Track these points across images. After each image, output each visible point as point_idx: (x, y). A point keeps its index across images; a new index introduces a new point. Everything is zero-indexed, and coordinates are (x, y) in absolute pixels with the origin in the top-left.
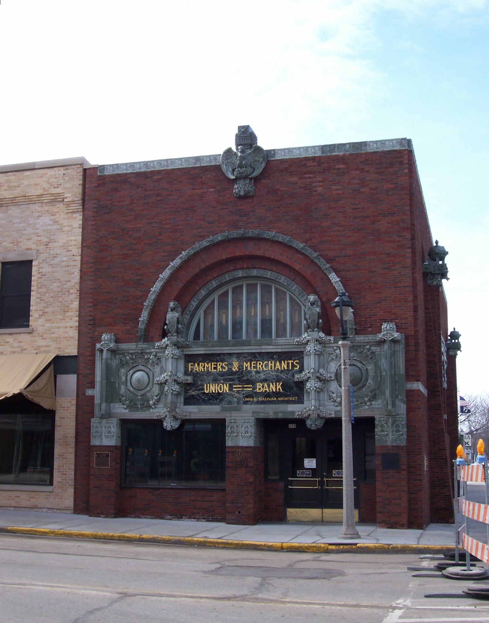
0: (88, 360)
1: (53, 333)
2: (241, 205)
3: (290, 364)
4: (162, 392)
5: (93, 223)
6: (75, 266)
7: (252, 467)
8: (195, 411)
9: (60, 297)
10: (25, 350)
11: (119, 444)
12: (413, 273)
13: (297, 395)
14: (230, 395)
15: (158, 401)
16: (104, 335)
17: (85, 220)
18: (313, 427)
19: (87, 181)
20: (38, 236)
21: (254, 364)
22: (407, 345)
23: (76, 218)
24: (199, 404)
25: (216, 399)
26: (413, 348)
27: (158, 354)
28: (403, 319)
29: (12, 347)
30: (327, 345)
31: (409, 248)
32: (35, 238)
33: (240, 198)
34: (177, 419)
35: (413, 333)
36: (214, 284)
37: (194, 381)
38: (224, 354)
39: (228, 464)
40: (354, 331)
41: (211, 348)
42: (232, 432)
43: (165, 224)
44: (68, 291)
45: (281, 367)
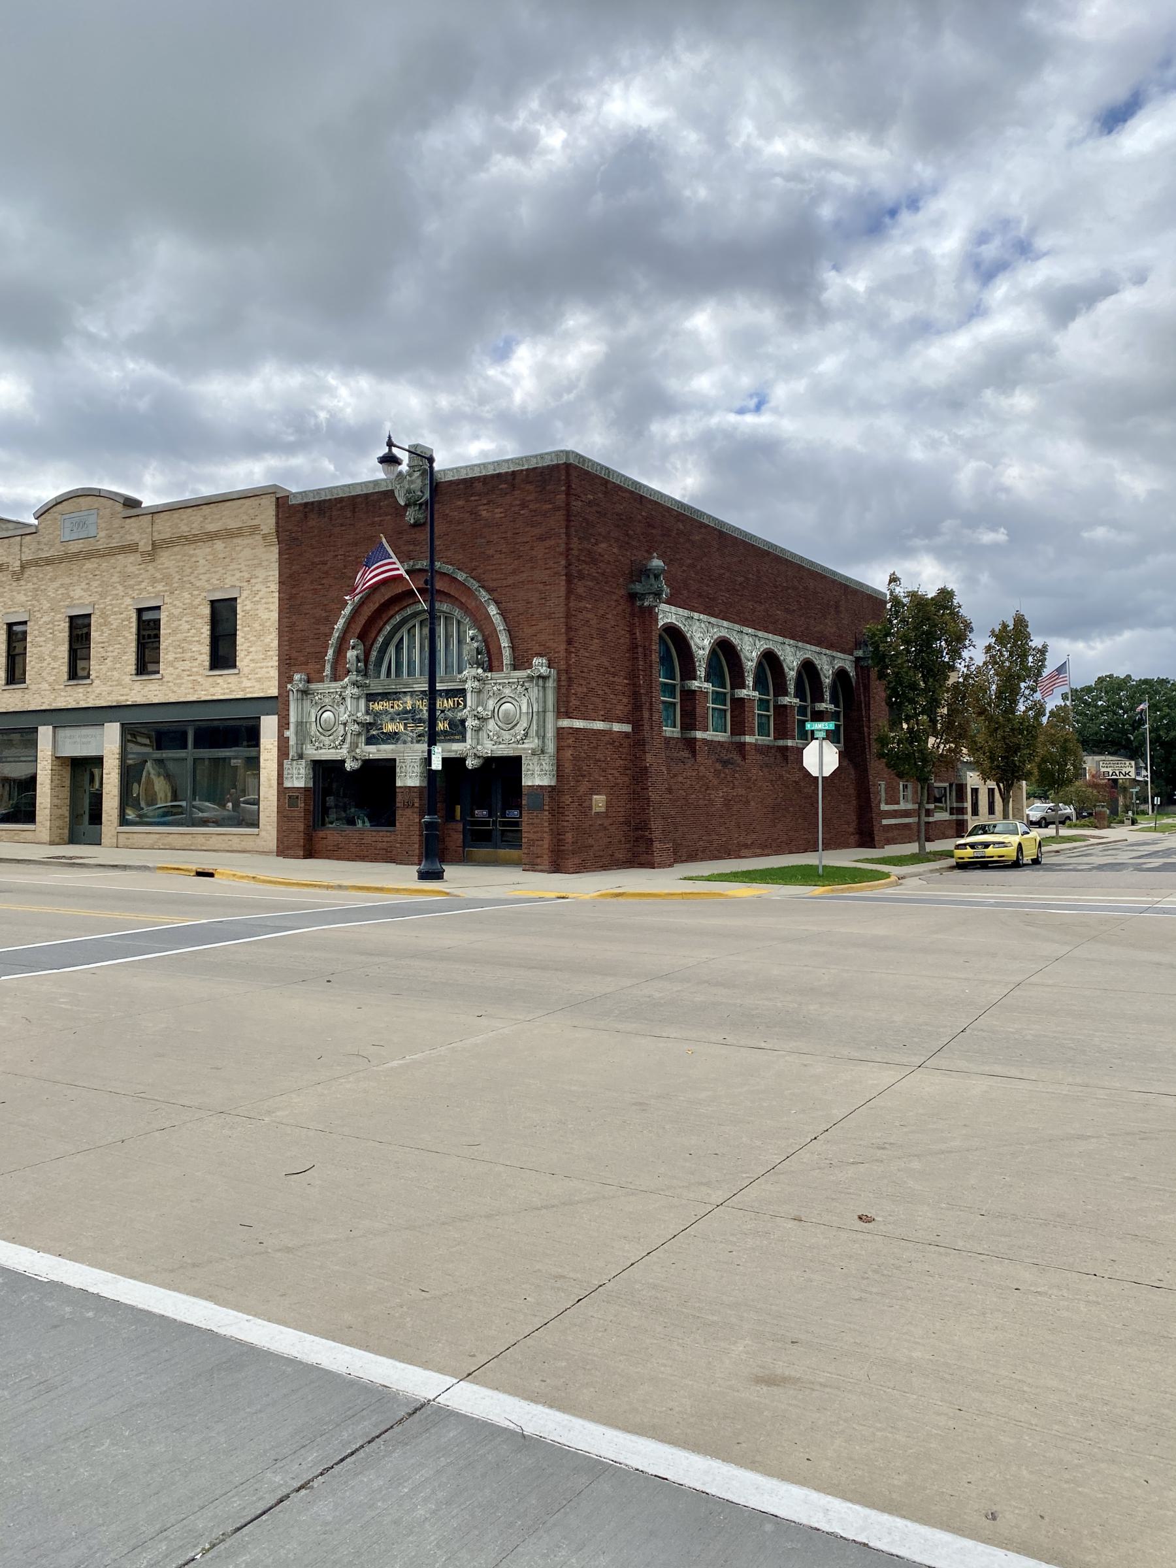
8: (374, 752)
15: (343, 741)
17: (280, 553)
22: (559, 680)
32: (238, 575)
39: (398, 805)
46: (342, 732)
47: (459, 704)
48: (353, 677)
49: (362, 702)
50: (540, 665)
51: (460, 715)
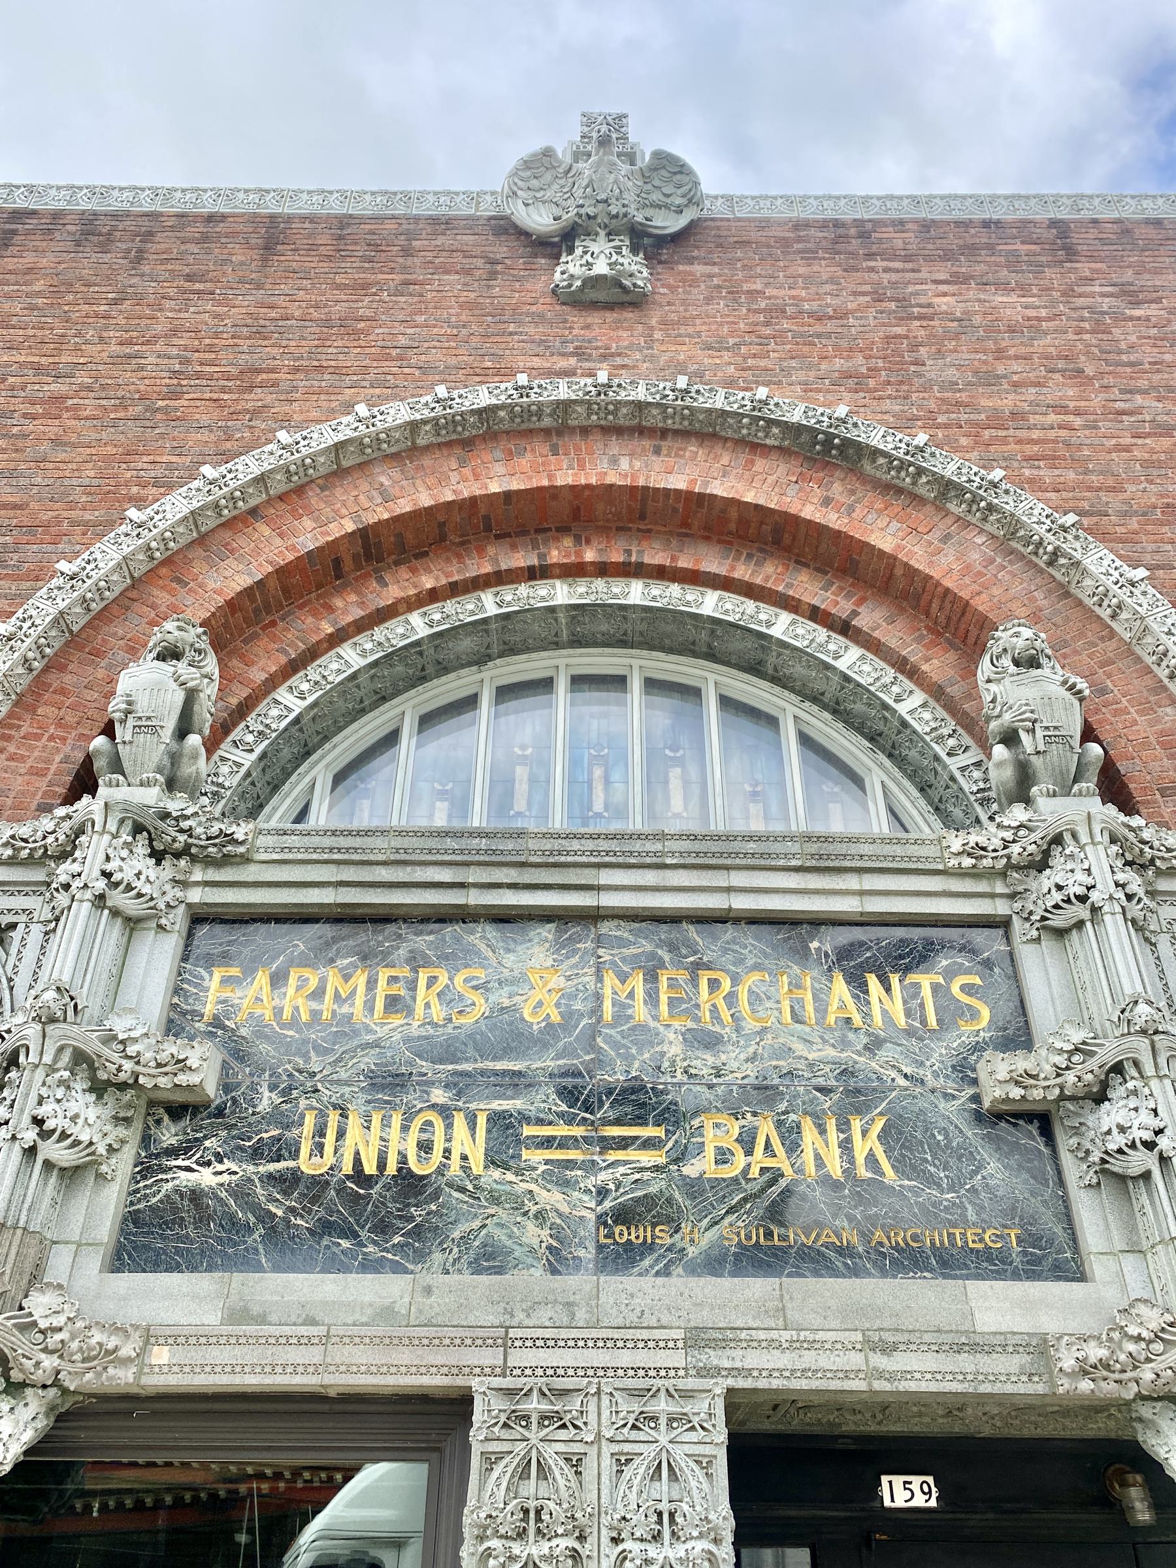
2: (587, 327)
3: (926, 992)
14: (495, 1200)
21: (673, 984)
24: (246, 1263)
25: (383, 1228)
37: (227, 1088)
42: (531, 1520)
45: (867, 1015)
49: (157, 957)
51: (999, 1077)
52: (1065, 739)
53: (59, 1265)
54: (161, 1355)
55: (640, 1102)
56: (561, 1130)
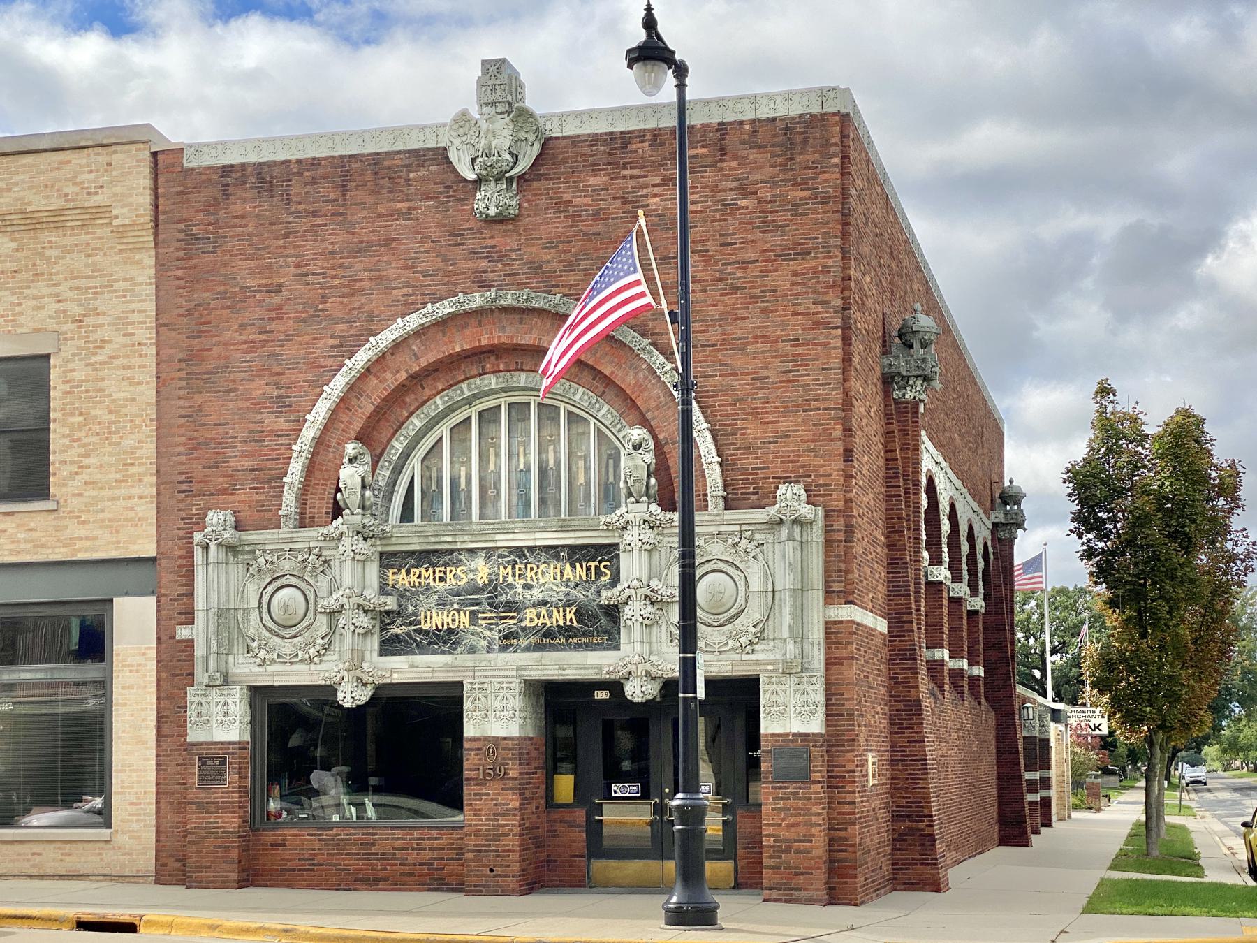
0: (180, 566)
1: (103, 511)
2: (492, 237)
4: (333, 630)
5: (179, 273)
6: (145, 366)
7: (516, 779)
8: (404, 669)
9: (115, 433)
10: (42, 546)
11: (247, 738)
12: (845, 380)
13: (606, 632)
16: (210, 513)
17: (160, 265)
18: (638, 699)
19: (161, 180)
20: (59, 301)
22: (828, 529)
23: (140, 262)
25: (445, 642)
26: (842, 536)
27: (325, 553)
28: (822, 475)
29: (13, 542)
30: (665, 531)
31: (837, 327)
33: (489, 221)
34: (365, 685)
35: (841, 503)
36: (440, 403)
38: (459, 551)
39: (467, 774)
40: (721, 501)
41: (432, 539)
42: (477, 709)
43: (334, 278)
44: (132, 421)
46: (324, 629)
47: (599, 573)
48: (352, 518)
49: (373, 570)
50: (791, 496)
51: (608, 596)
52: (640, 481)
53: (367, 654)
54: (395, 676)
55: (510, 606)
56: (489, 615)
